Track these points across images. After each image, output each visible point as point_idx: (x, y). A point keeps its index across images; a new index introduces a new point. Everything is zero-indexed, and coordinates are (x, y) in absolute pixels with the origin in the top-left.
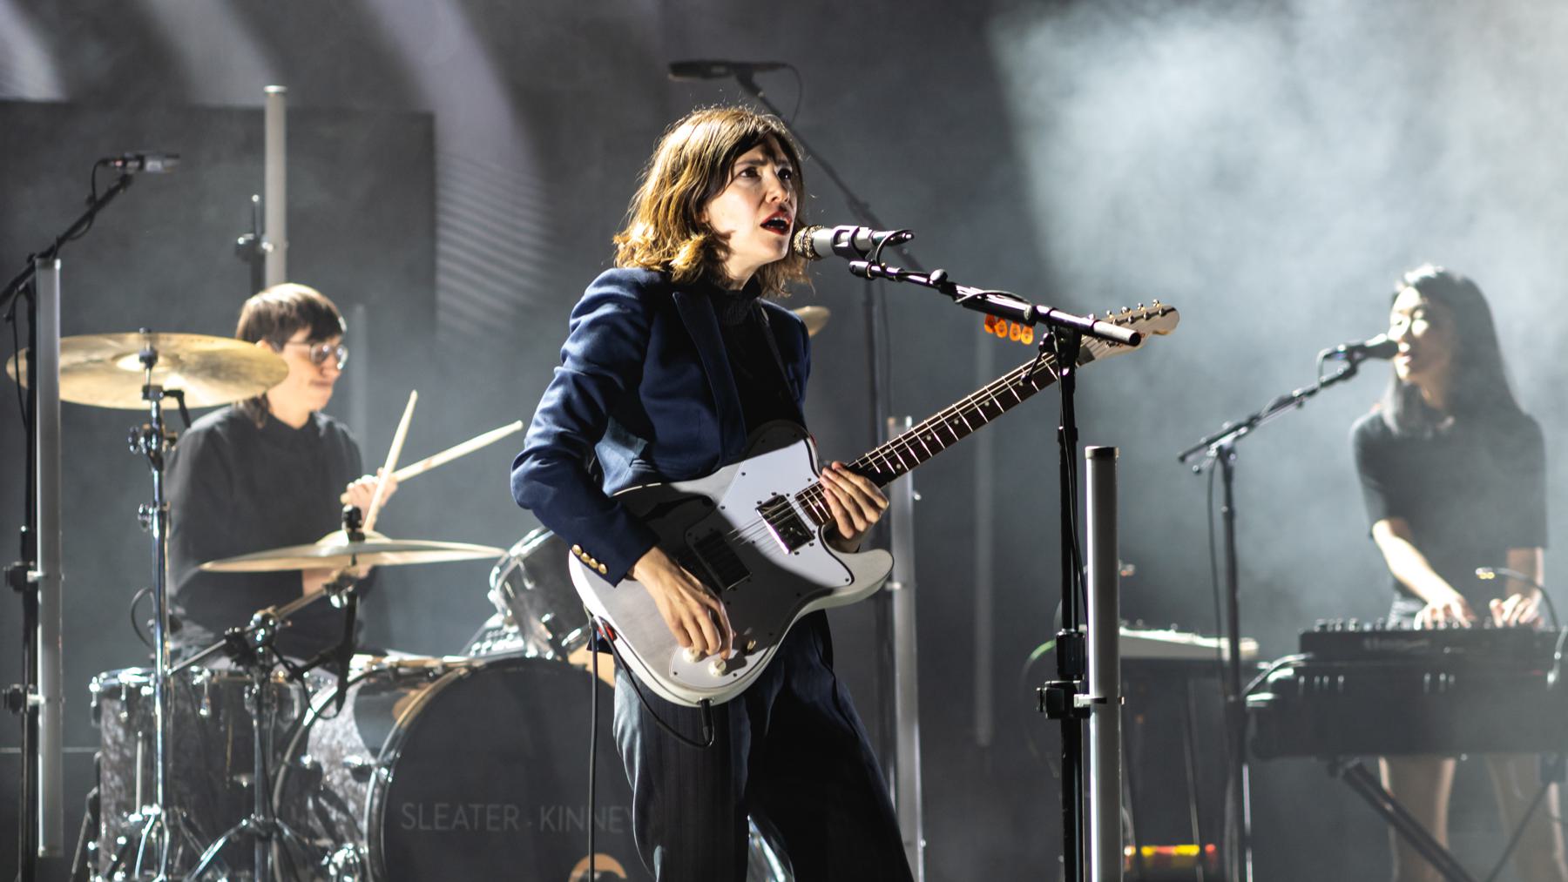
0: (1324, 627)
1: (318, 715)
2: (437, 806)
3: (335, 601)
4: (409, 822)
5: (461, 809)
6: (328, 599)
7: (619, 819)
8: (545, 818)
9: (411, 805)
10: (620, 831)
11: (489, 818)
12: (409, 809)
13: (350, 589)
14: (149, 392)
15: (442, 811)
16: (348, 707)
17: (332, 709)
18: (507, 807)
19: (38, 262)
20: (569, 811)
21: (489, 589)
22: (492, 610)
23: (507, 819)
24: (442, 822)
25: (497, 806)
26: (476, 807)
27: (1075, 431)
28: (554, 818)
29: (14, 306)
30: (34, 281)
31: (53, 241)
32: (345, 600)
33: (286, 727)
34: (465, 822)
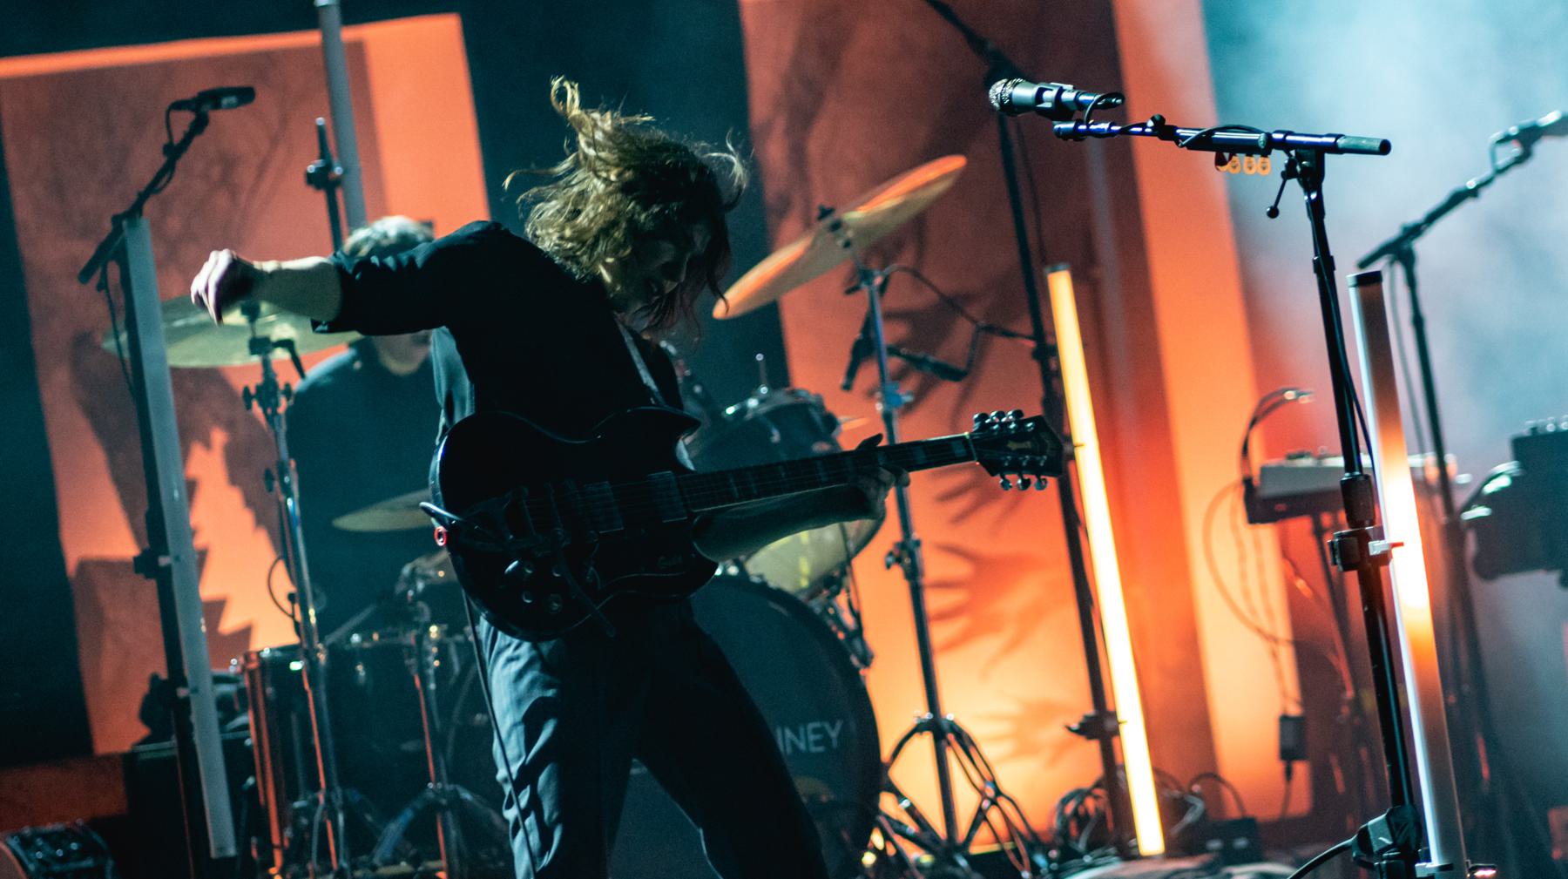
0: (1534, 429)
7: (818, 737)
10: (820, 749)
14: (260, 346)
19: (125, 223)
27: (1331, 259)
29: (104, 273)
30: (124, 243)
31: (134, 198)
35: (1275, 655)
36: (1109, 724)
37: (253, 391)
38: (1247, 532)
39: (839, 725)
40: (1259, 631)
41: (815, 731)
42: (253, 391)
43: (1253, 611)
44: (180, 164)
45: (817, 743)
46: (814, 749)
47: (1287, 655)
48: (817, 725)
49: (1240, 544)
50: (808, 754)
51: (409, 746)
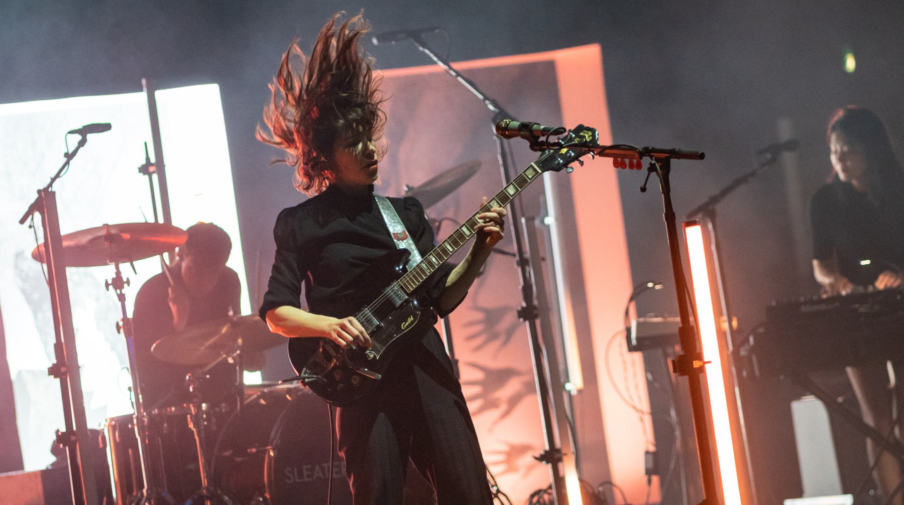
2: (305, 467)
4: (289, 478)
5: (317, 467)
9: (290, 469)
12: (290, 472)
24: (308, 476)
34: (321, 474)
35: (642, 420)
36: (557, 455)
37: (110, 282)
40: (634, 407)
42: (110, 282)
43: (631, 397)
44: (71, 162)
47: (648, 420)
49: (624, 362)
51: (191, 466)
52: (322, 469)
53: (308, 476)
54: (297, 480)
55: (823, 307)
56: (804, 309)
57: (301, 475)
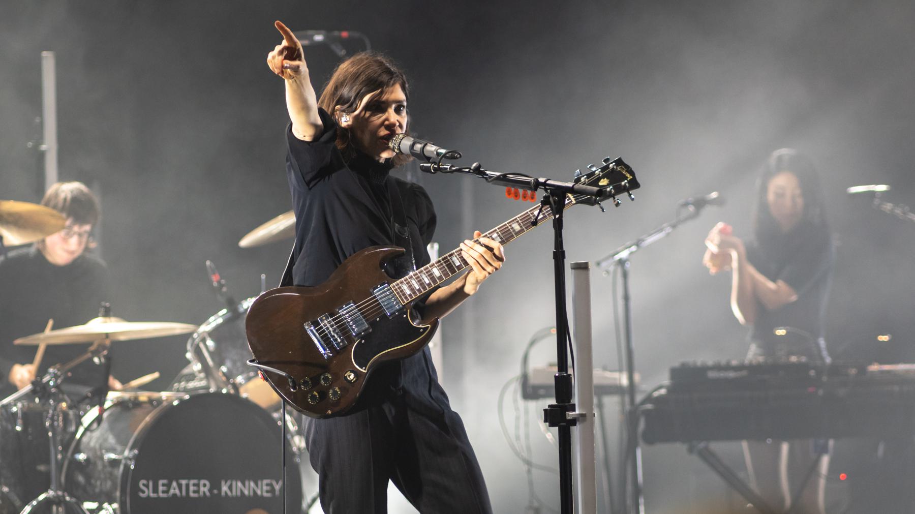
1: (87, 429)
2: (161, 482)
3: (96, 360)
4: (143, 492)
5: (174, 484)
6: (91, 359)
7: (268, 488)
8: (225, 488)
9: (144, 482)
10: (269, 495)
11: (192, 488)
12: (144, 485)
13: (105, 352)
15: (163, 485)
16: (105, 425)
17: (95, 425)
18: (202, 482)
20: (239, 484)
21: (186, 351)
22: (188, 362)
23: (202, 489)
24: (163, 492)
25: (195, 481)
26: (184, 482)
28: (230, 488)
32: (103, 360)
33: (67, 437)
34: (177, 492)
38: (521, 403)
39: (281, 483)
41: (267, 485)
45: (267, 492)
46: (265, 494)
48: (268, 481)
49: (517, 409)
50: (262, 497)
51: (42, 468)
52: (180, 486)
53: (163, 492)
54: (152, 495)
55: (731, 374)
56: (712, 374)
57: (155, 490)
